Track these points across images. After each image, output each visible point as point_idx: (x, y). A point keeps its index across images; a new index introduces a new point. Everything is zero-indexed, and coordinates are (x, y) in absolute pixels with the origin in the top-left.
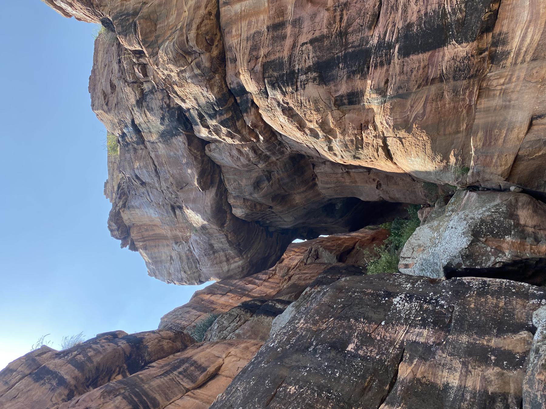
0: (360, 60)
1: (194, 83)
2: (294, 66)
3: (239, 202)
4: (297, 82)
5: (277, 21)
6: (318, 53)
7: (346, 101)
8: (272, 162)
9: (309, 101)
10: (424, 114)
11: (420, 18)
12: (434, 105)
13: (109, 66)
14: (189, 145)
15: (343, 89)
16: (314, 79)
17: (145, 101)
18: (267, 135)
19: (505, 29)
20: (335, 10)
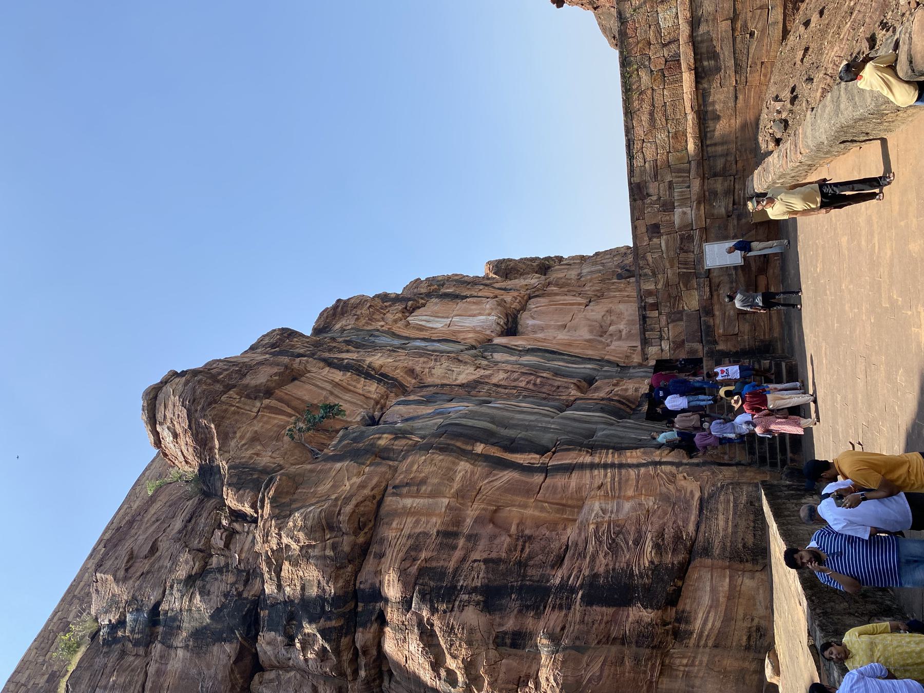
0: (537, 597)
1: (316, 566)
2: (458, 581)
4: (455, 600)
5: (450, 529)
6: (490, 576)
7: (508, 641)
9: (463, 629)
10: (600, 678)
11: (607, 571)
13: (164, 522)
14: (235, 662)
15: (510, 624)
16: (478, 603)
17: (203, 580)
18: (373, 672)
19: (688, 608)
20: (518, 539)
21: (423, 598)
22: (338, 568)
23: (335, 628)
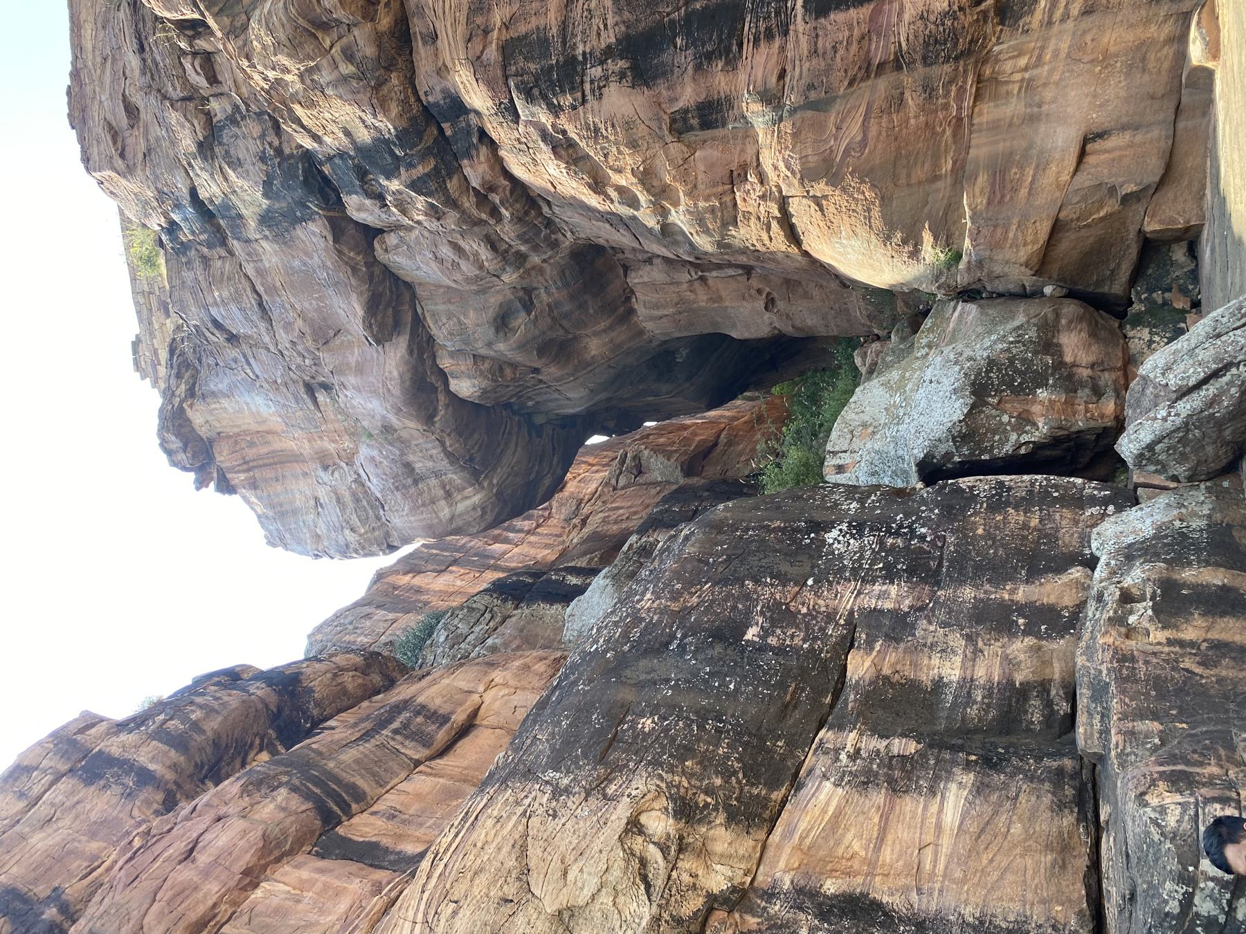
1: (341, 97)
2: (574, 47)
3: (465, 365)
4: (582, 82)
6: (626, 15)
7: (695, 122)
8: (533, 268)
9: (613, 126)
10: (864, 143)
12: (885, 119)
13: (114, 60)
14: (336, 240)
15: (688, 94)
16: (622, 75)
17: (220, 144)
18: (518, 206)
21: (529, 97)
22: (377, 88)
23: (426, 175)
